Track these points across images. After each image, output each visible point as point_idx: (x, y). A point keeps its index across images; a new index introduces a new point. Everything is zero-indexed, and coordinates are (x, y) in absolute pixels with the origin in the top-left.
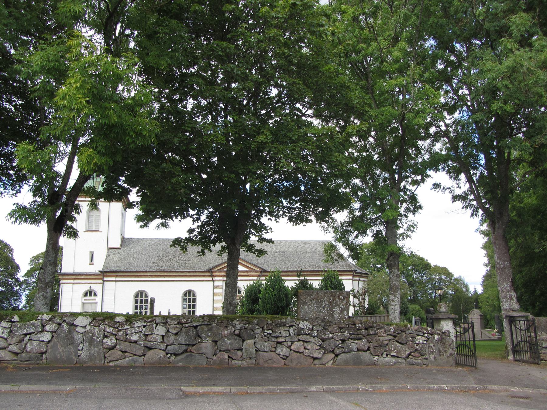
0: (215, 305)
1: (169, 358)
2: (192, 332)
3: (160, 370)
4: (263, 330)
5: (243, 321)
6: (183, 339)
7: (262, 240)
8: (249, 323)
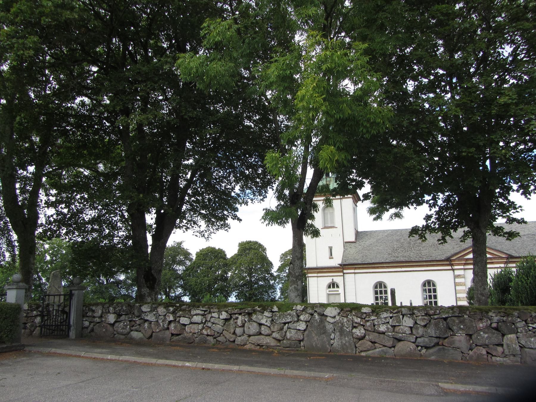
0: (458, 295)
1: (420, 351)
2: (442, 324)
3: (411, 363)
4: (526, 323)
5: (500, 312)
6: (433, 331)
7: (511, 220)
8: (508, 315)
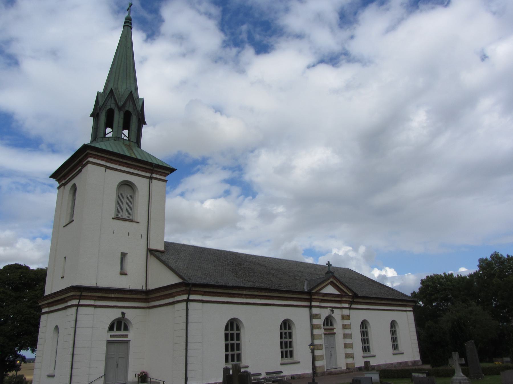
0: (316, 342)
